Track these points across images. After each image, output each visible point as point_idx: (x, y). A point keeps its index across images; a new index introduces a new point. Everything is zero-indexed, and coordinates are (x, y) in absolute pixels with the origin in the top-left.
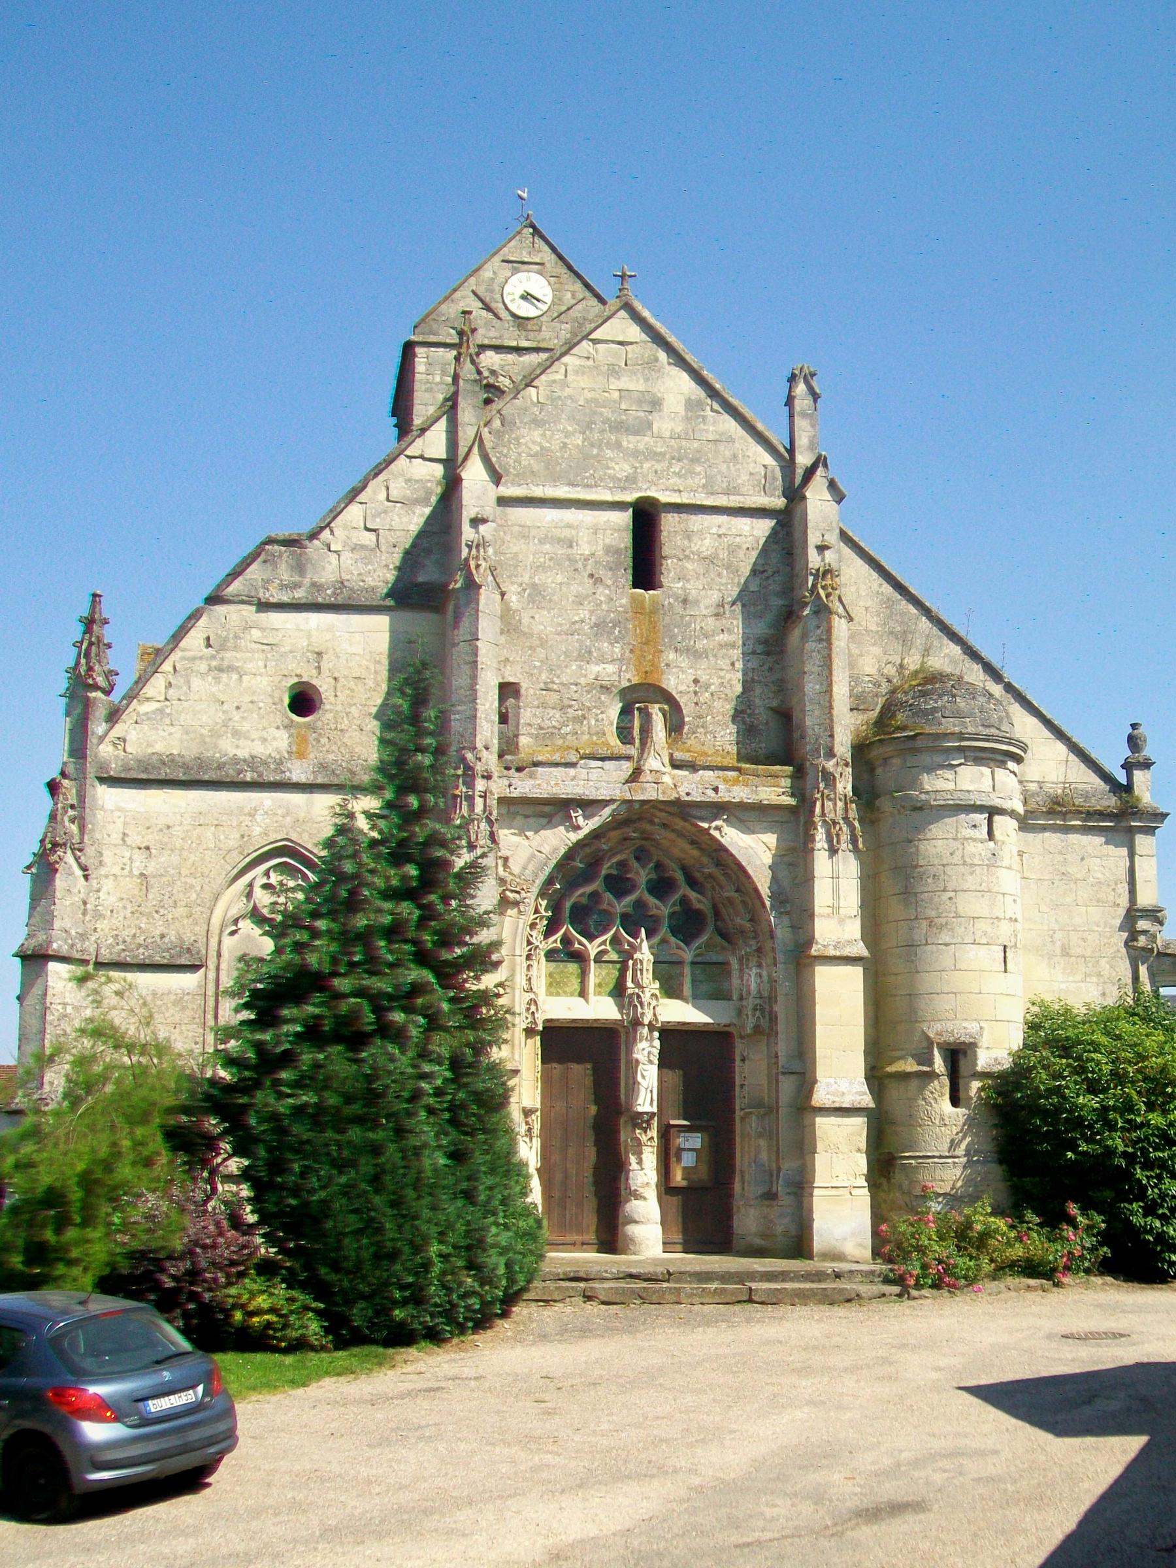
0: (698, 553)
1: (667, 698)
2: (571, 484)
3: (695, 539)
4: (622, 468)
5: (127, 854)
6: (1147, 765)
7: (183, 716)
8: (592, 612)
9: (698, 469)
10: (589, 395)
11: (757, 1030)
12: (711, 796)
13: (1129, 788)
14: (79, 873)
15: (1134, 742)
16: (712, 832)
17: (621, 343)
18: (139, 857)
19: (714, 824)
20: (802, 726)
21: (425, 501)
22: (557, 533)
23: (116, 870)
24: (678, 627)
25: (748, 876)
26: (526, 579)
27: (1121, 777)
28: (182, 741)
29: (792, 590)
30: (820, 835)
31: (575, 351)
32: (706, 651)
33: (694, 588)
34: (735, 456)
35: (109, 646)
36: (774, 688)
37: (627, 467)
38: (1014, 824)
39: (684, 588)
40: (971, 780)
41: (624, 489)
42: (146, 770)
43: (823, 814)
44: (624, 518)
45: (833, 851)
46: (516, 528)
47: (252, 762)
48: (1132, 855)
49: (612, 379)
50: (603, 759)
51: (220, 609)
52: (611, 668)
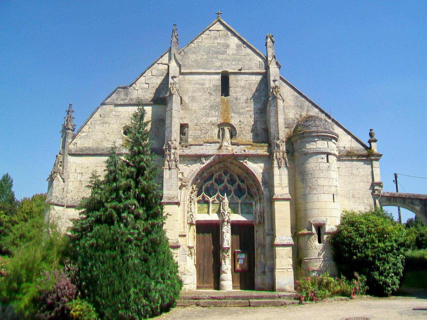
0: (240, 86)
3: (239, 82)
4: (218, 64)
17: (218, 31)
20: (270, 133)
24: (235, 106)
30: (275, 162)
33: (239, 95)
34: (251, 59)
37: (220, 63)
39: (236, 96)
43: (276, 156)
44: (219, 77)
49: (215, 40)
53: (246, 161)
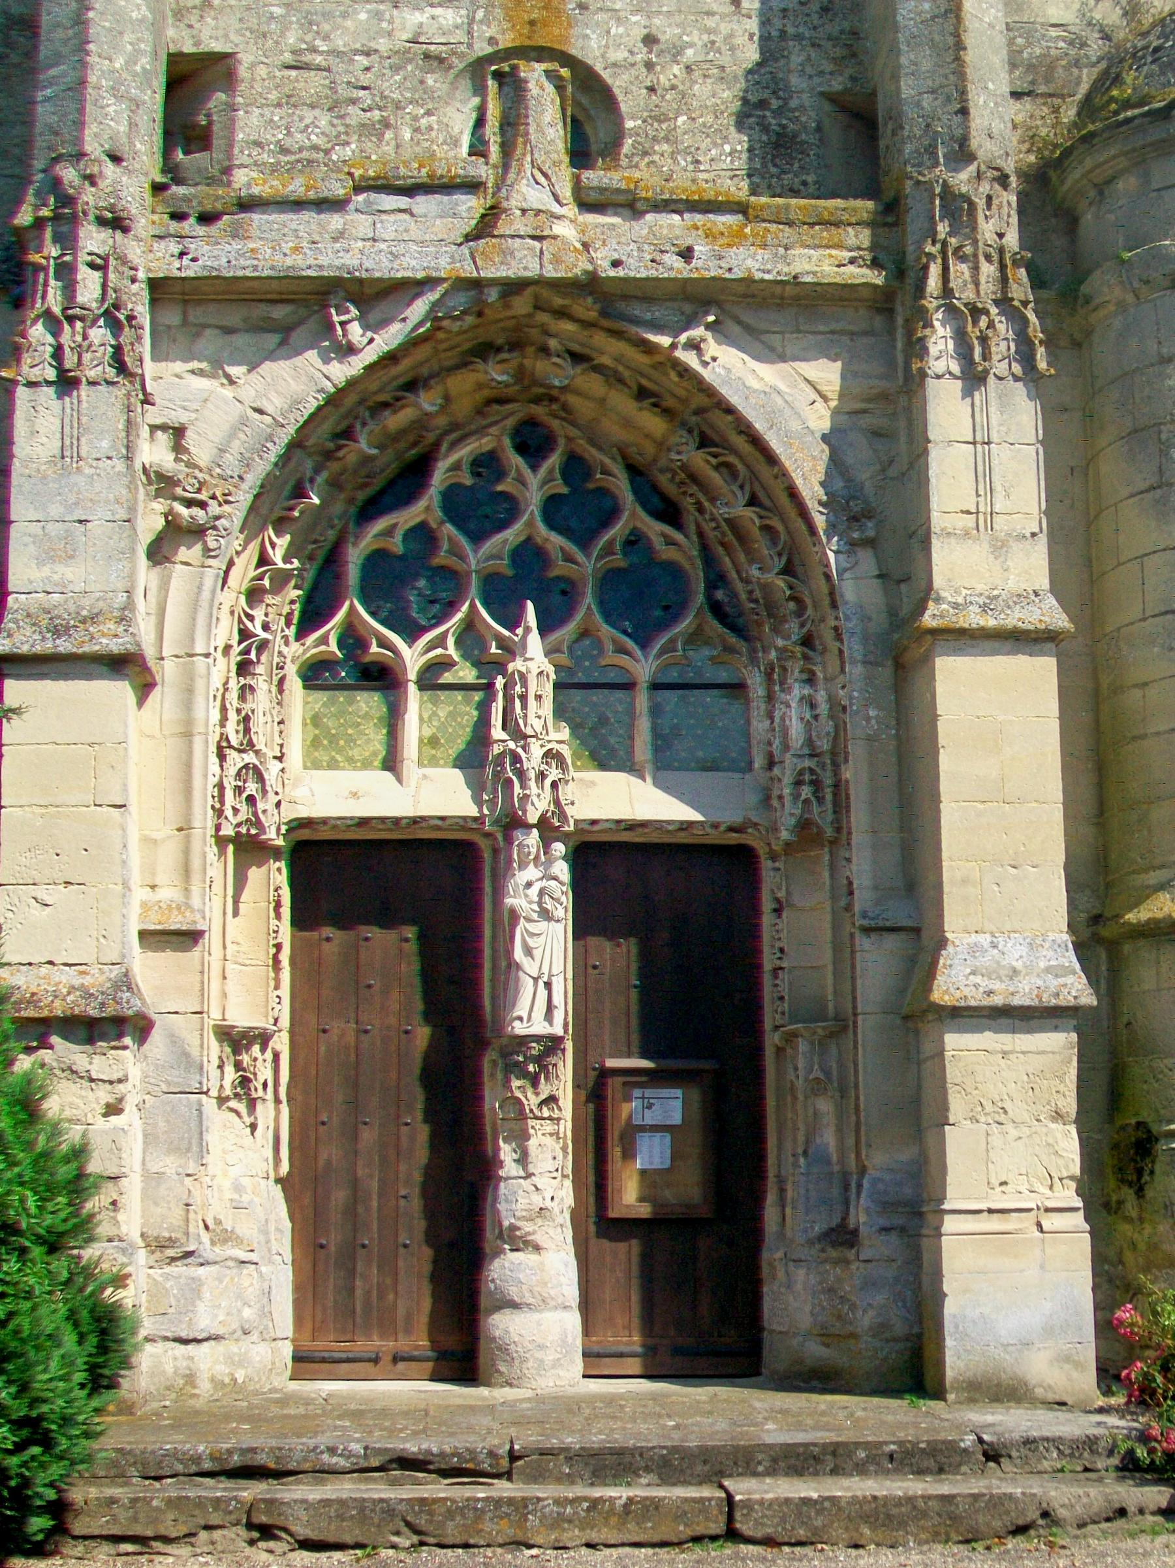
16: (679, 354)
19: (683, 338)
50: (410, 191)
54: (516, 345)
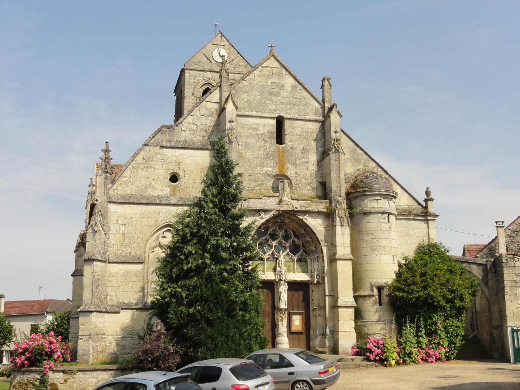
0: (296, 134)
1: (288, 178)
2: (256, 111)
3: (295, 129)
5: (118, 227)
6: (432, 200)
7: (136, 183)
8: (264, 151)
9: (295, 107)
10: (262, 84)
11: (318, 282)
12: (303, 209)
13: (426, 208)
14: (103, 232)
15: (427, 193)
17: (271, 67)
18: (122, 228)
21: (211, 115)
22: (253, 126)
23: (115, 232)
25: (314, 233)
26: (244, 140)
27: (424, 204)
28: (136, 190)
29: (325, 145)
31: (257, 70)
32: (299, 164)
33: (295, 144)
34: (306, 104)
35: (111, 159)
36: (320, 176)
38: (394, 218)
39: (292, 144)
40: (383, 204)
41: (273, 113)
42: (124, 199)
44: (274, 122)
45: (342, 226)
46: (240, 125)
47: (159, 197)
48: (428, 227)
50: (270, 197)
51: (147, 148)
52: (270, 169)
53: (305, 217)
54: (281, 216)
